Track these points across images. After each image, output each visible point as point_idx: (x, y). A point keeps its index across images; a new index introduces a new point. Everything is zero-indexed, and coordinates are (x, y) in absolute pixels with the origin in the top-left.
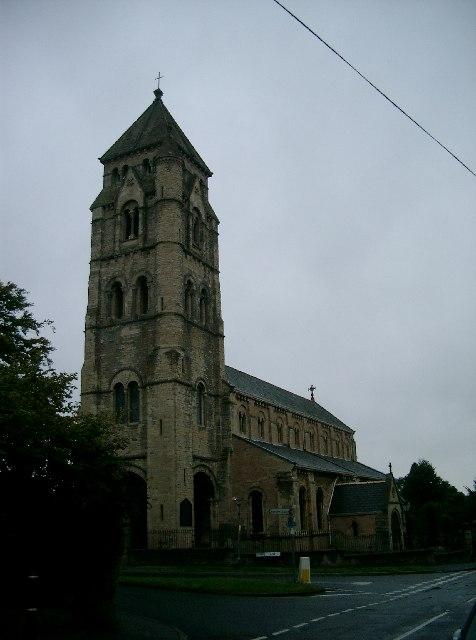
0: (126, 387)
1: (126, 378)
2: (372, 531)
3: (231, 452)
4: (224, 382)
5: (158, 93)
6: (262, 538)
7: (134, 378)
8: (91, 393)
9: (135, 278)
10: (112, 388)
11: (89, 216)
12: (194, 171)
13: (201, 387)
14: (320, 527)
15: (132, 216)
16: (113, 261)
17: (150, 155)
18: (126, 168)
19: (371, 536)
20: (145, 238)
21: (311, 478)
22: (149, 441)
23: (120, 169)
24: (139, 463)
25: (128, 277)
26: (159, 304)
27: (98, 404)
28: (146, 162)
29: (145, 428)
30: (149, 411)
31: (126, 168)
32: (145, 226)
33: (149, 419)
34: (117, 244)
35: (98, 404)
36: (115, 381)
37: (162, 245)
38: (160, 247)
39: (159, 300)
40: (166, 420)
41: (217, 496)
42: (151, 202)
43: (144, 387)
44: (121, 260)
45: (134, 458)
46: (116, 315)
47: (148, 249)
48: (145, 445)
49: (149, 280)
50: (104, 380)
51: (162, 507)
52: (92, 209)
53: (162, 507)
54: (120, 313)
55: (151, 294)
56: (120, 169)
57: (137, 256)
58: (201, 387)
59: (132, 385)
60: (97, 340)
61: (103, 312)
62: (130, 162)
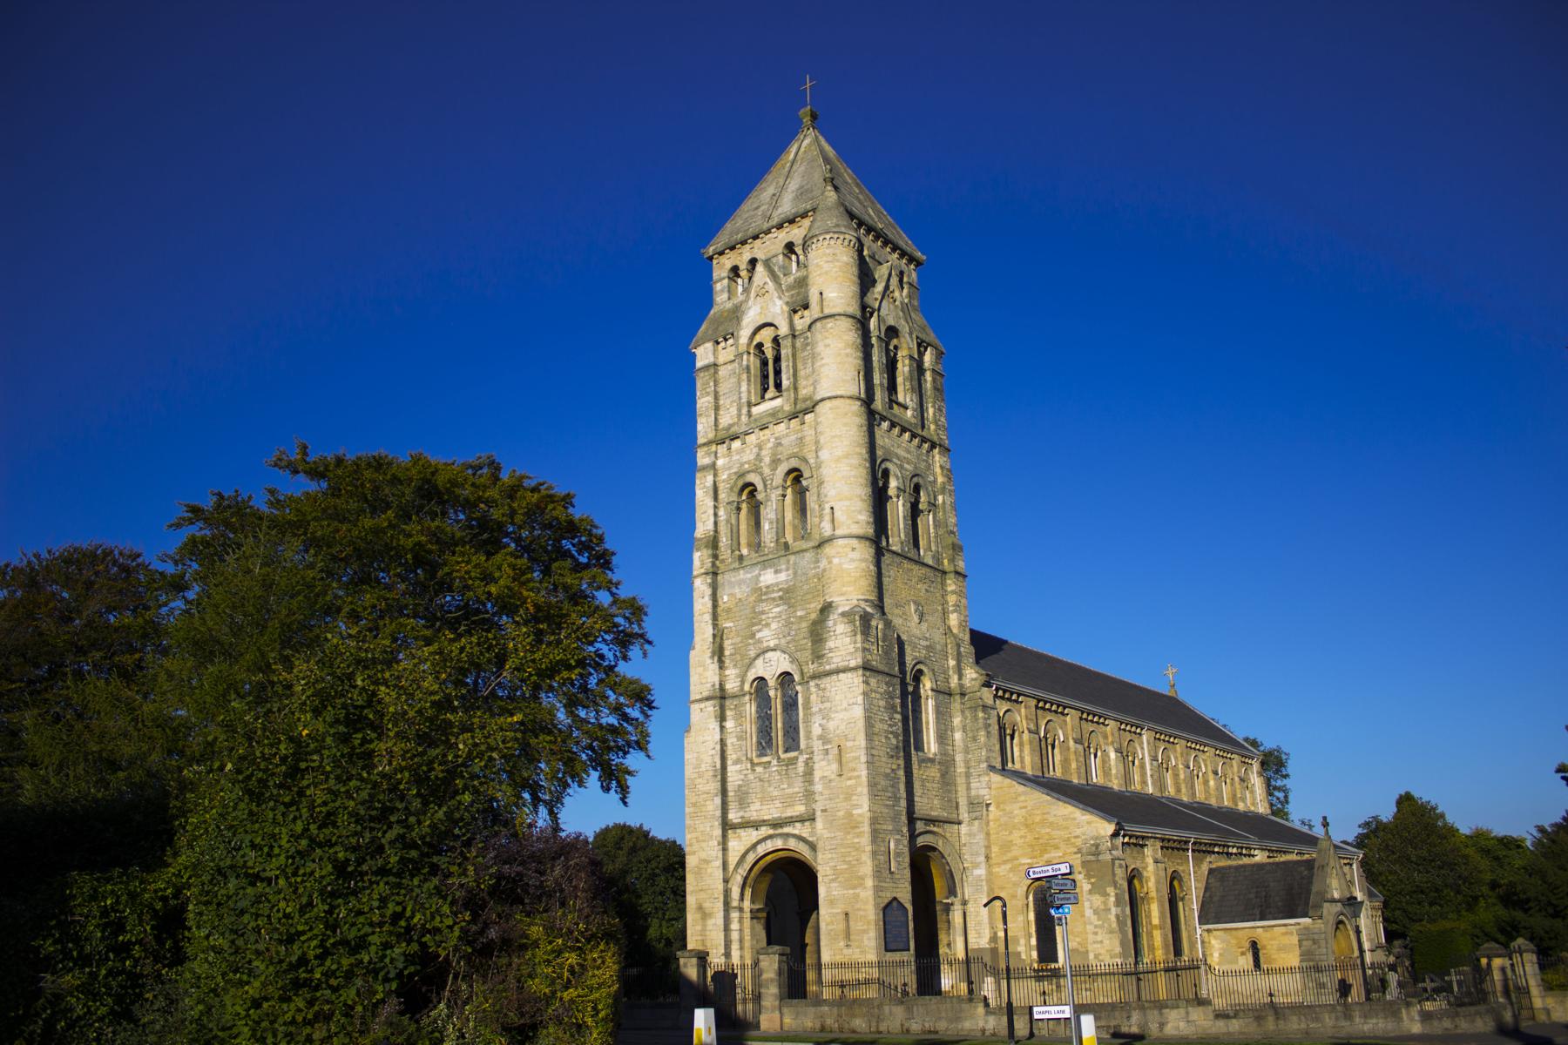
0: (772, 683)
1: (772, 666)
3: (988, 805)
6: (1056, 974)
7: (786, 665)
8: (707, 699)
10: (747, 687)
15: (769, 354)
16: (736, 444)
17: (796, 234)
18: (753, 262)
21: (1151, 852)
22: (818, 787)
23: (743, 266)
24: (797, 829)
25: (767, 471)
26: (827, 518)
27: (722, 718)
28: (790, 248)
29: (809, 764)
30: (816, 730)
31: (753, 262)
32: (795, 375)
33: (817, 745)
34: (745, 410)
35: (722, 718)
36: (751, 675)
37: (828, 404)
38: (818, 408)
39: (827, 510)
40: (849, 744)
42: (800, 323)
43: (804, 682)
44: (751, 439)
45: (791, 821)
46: (749, 545)
47: (802, 410)
48: (809, 796)
49: (806, 474)
50: (731, 672)
51: (847, 914)
53: (847, 914)
54: (757, 546)
55: (811, 499)
56: (743, 266)
59: (786, 677)
61: (724, 540)
62: (759, 249)
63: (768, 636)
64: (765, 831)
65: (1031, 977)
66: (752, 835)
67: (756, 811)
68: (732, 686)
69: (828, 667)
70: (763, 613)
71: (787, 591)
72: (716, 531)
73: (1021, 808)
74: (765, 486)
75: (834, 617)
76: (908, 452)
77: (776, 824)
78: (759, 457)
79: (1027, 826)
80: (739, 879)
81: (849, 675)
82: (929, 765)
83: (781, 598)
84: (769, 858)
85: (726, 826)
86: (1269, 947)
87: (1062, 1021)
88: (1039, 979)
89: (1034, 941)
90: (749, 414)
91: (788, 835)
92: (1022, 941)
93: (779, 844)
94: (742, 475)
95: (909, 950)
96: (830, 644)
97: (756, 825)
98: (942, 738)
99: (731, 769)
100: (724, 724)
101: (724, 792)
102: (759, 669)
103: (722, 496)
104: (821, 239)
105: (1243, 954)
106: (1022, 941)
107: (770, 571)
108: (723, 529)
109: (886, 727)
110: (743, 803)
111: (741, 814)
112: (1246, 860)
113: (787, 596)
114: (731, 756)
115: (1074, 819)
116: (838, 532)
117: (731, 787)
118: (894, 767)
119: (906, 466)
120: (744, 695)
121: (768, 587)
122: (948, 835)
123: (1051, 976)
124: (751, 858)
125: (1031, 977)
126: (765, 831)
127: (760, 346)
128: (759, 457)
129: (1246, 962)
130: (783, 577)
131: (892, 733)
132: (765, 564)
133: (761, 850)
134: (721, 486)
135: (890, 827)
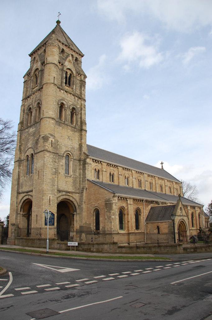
2: (166, 231)
4: (84, 153)
5: (58, 22)
7: (32, 152)
9: (36, 103)
11: (23, 80)
12: (71, 52)
13: (68, 156)
14: (137, 227)
16: (29, 99)
19: (166, 234)
20: (40, 85)
21: (130, 202)
22: (34, 182)
25: (34, 104)
27: (19, 166)
30: (35, 168)
36: (26, 155)
41: (78, 211)
44: (32, 97)
49: (40, 103)
52: (24, 77)
57: (37, 93)
58: (68, 156)
59: (32, 154)
60: (21, 136)
62: (39, 52)
63: (30, 145)
64: (25, 194)
65: (93, 234)
66: (23, 195)
67: (25, 189)
68: (22, 158)
69: (38, 151)
70: (29, 139)
71: (34, 133)
72: (23, 120)
73: (93, 190)
74: (33, 107)
75: (41, 138)
76: (71, 99)
77: (27, 192)
78: (32, 101)
79: (94, 194)
80: (20, 206)
81: (42, 153)
82: (69, 178)
83: (33, 135)
84: (26, 201)
85: (19, 193)
86: (161, 228)
87: (75, 247)
88: (95, 234)
89: (95, 225)
90: (32, 91)
91: (29, 195)
92: (92, 224)
93: (27, 197)
94: (29, 106)
95: (53, 225)
96: (39, 145)
97: (24, 193)
98: (74, 171)
99: (21, 178)
100: (20, 167)
101: (18, 184)
102: (27, 154)
103: (25, 112)
104: (48, 45)
105: (155, 229)
106: (92, 224)
107: (32, 128)
108: (25, 120)
109: (52, 166)
110: (22, 187)
111: (21, 190)
112: (165, 205)
113: (34, 134)
114: (21, 175)
115: (105, 192)
116: (44, 117)
117: (20, 183)
118: (54, 177)
119: (70, 102)
120: (24, 160)
121: (31, 132)
122: (74, 196)
123: (97, 234)
124: (22, 201)
125: (93, 234)
126: (25, 194)
127: (36, 75)
128: (32, 101)
129: (156, 231)
130: (34, 129)
131: (53, 168)
132: (31, 127)
133: (25, 198)
134: (26, 109)
135: (51, 193)
